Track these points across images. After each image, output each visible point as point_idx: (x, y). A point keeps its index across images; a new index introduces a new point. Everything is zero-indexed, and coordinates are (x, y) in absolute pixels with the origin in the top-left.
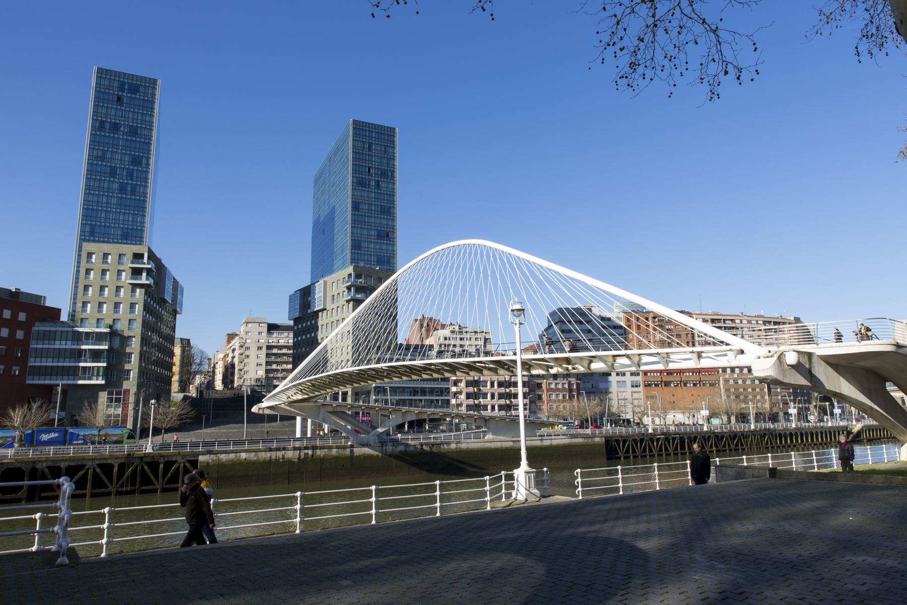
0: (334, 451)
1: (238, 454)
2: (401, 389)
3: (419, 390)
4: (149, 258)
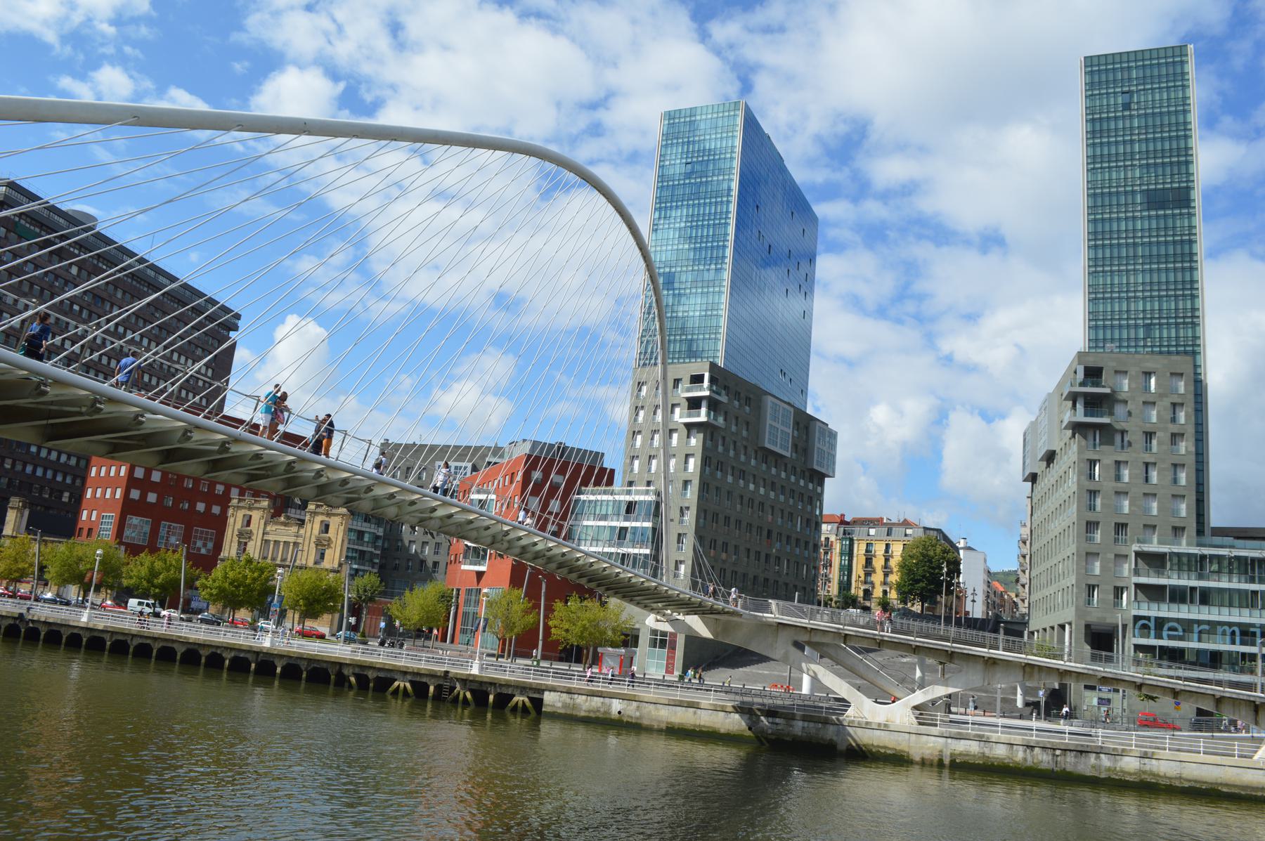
0: (800, 723)
1: (607, 700)
2: (1206, 627)
3: (1258, 631)
4: (712, 380)
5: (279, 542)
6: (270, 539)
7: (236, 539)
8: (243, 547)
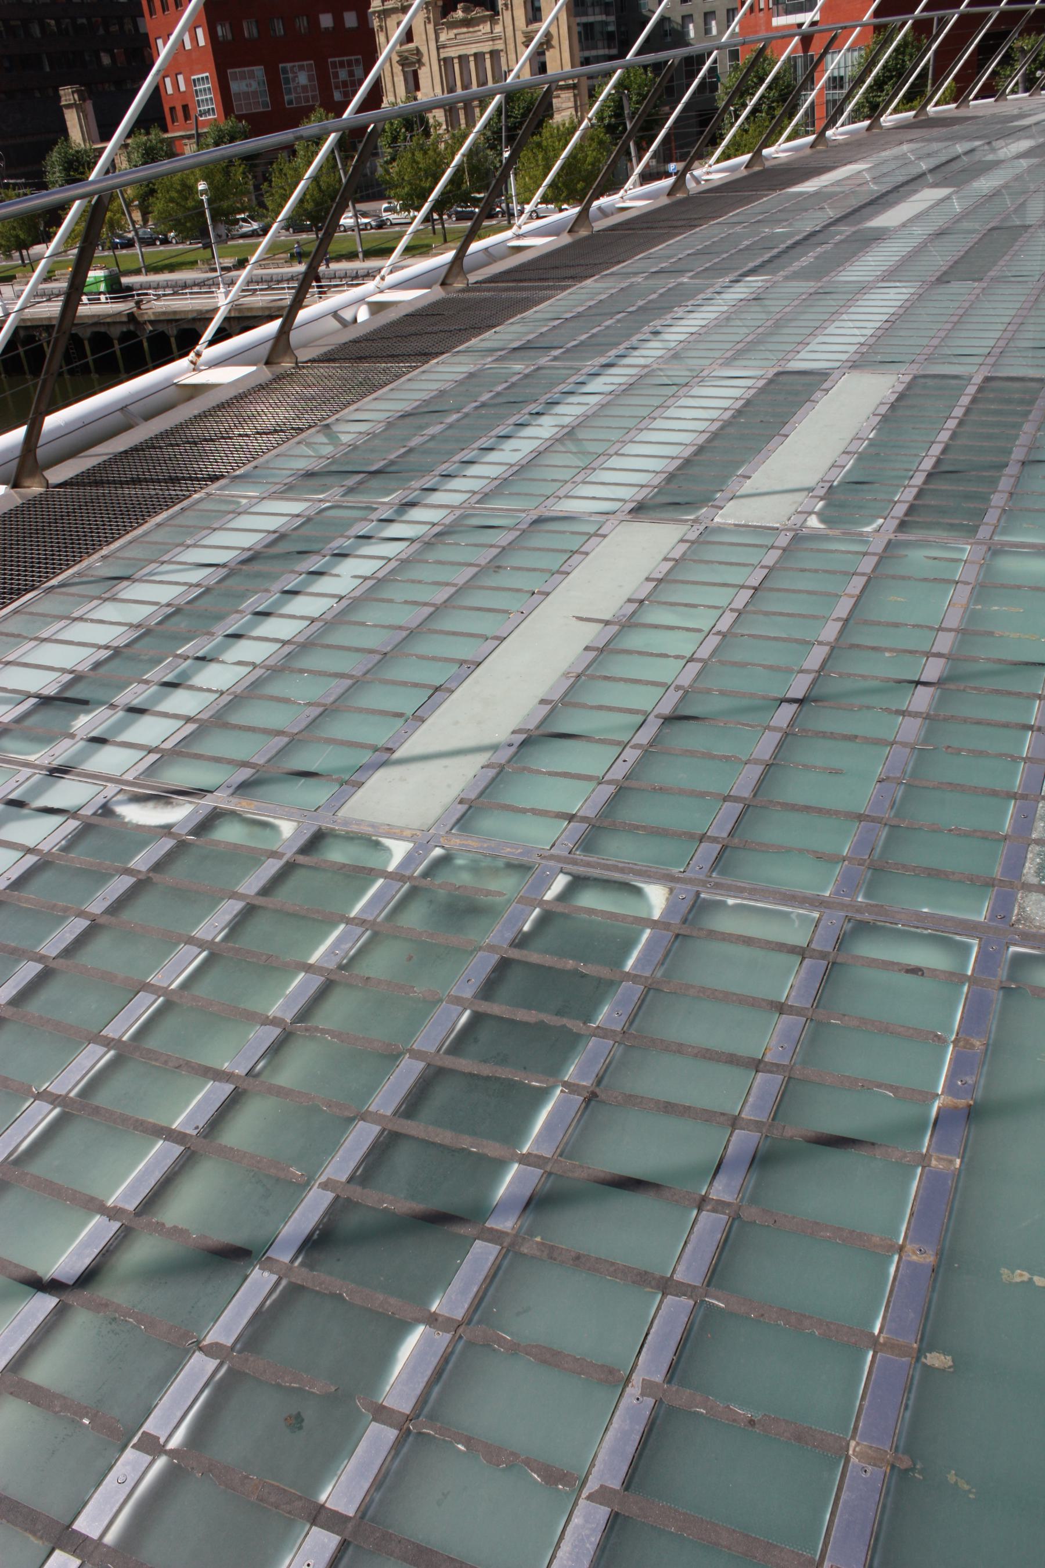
5: (467, 56)
6: (453, 55)
7: (398, 69)
8: (414, 83)
